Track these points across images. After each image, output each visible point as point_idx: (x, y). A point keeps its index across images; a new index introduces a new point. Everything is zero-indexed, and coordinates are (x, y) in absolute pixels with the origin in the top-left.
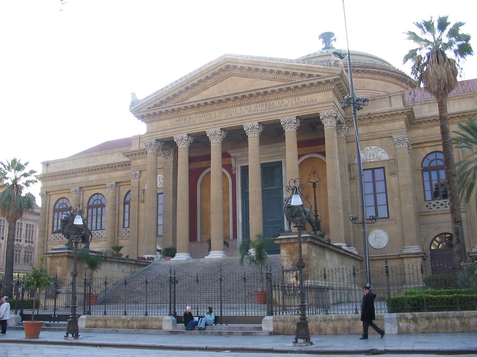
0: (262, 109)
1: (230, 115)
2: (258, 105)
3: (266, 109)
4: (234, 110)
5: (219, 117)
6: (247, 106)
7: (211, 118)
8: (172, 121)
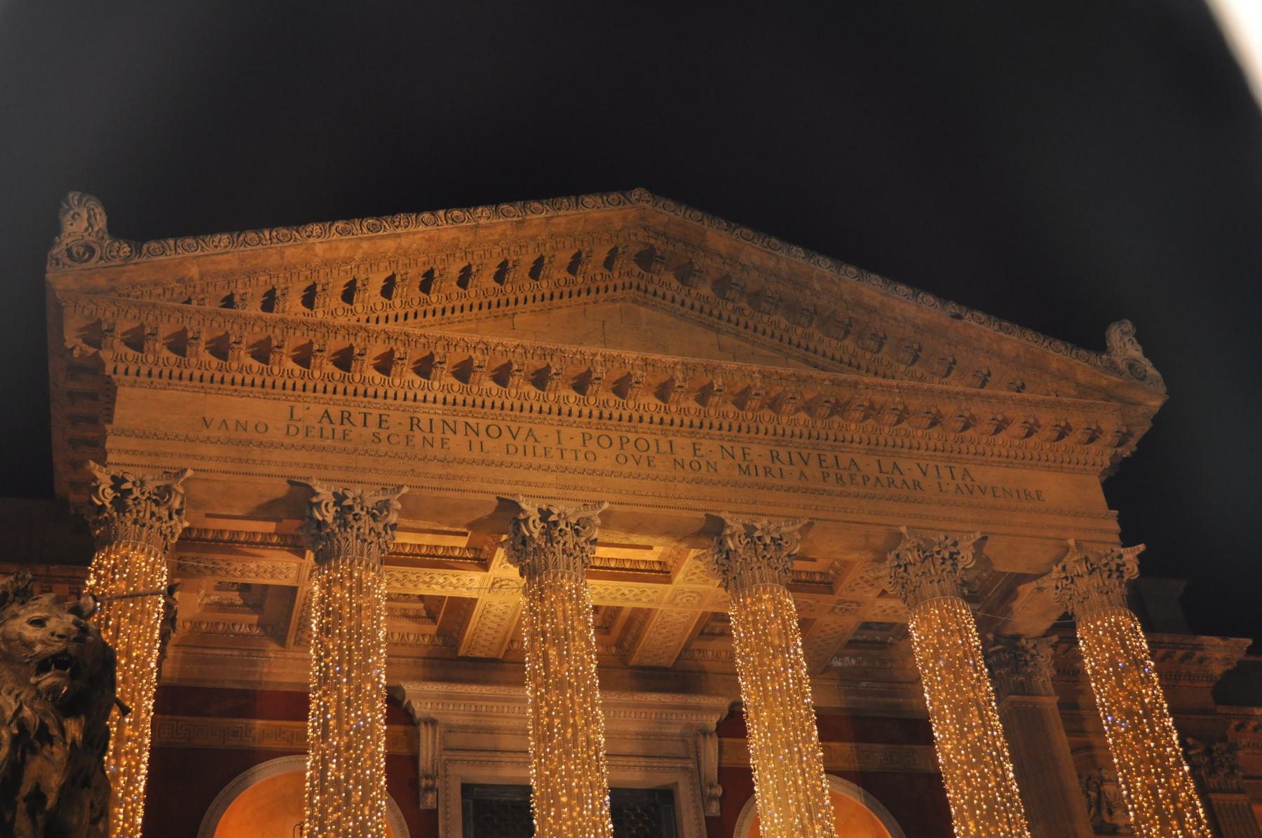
0: (802, 473)
1: (644, 463)
2: (784, 455)
3: (825, 477)
4: (664, 446)
5: (581, 456)
6: (727, 445)
7: (540, 451)
8: (299, 411)
